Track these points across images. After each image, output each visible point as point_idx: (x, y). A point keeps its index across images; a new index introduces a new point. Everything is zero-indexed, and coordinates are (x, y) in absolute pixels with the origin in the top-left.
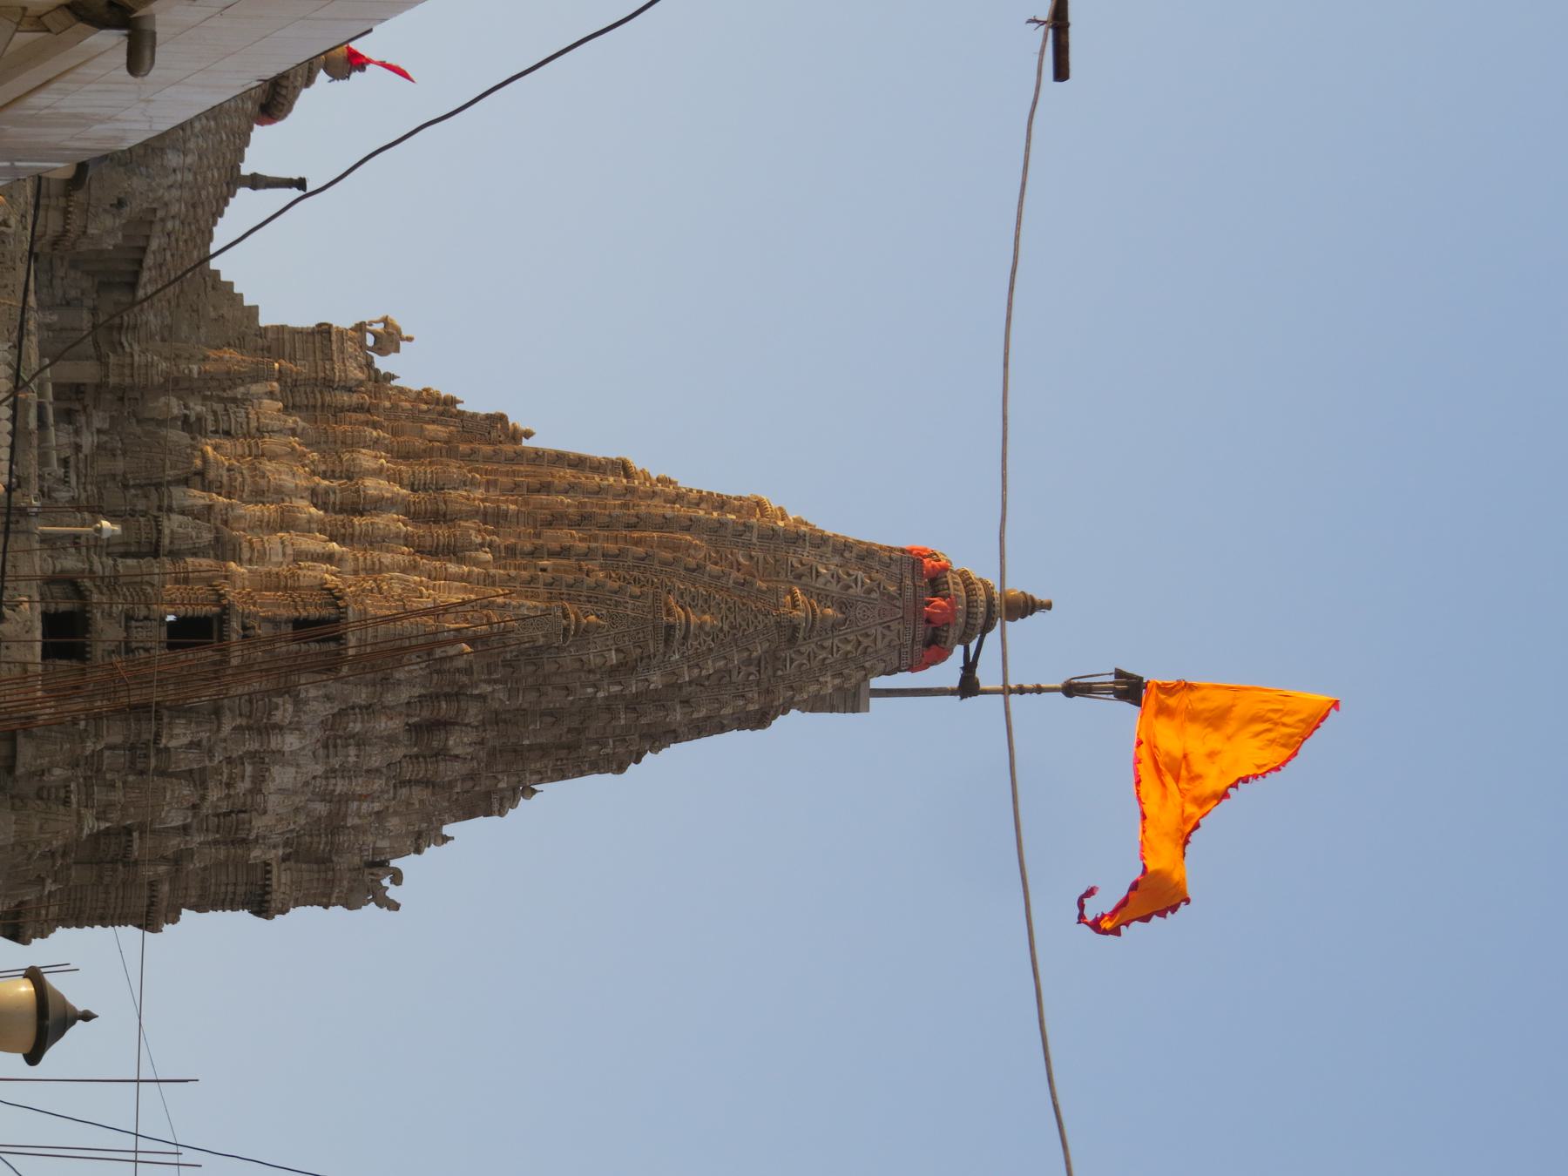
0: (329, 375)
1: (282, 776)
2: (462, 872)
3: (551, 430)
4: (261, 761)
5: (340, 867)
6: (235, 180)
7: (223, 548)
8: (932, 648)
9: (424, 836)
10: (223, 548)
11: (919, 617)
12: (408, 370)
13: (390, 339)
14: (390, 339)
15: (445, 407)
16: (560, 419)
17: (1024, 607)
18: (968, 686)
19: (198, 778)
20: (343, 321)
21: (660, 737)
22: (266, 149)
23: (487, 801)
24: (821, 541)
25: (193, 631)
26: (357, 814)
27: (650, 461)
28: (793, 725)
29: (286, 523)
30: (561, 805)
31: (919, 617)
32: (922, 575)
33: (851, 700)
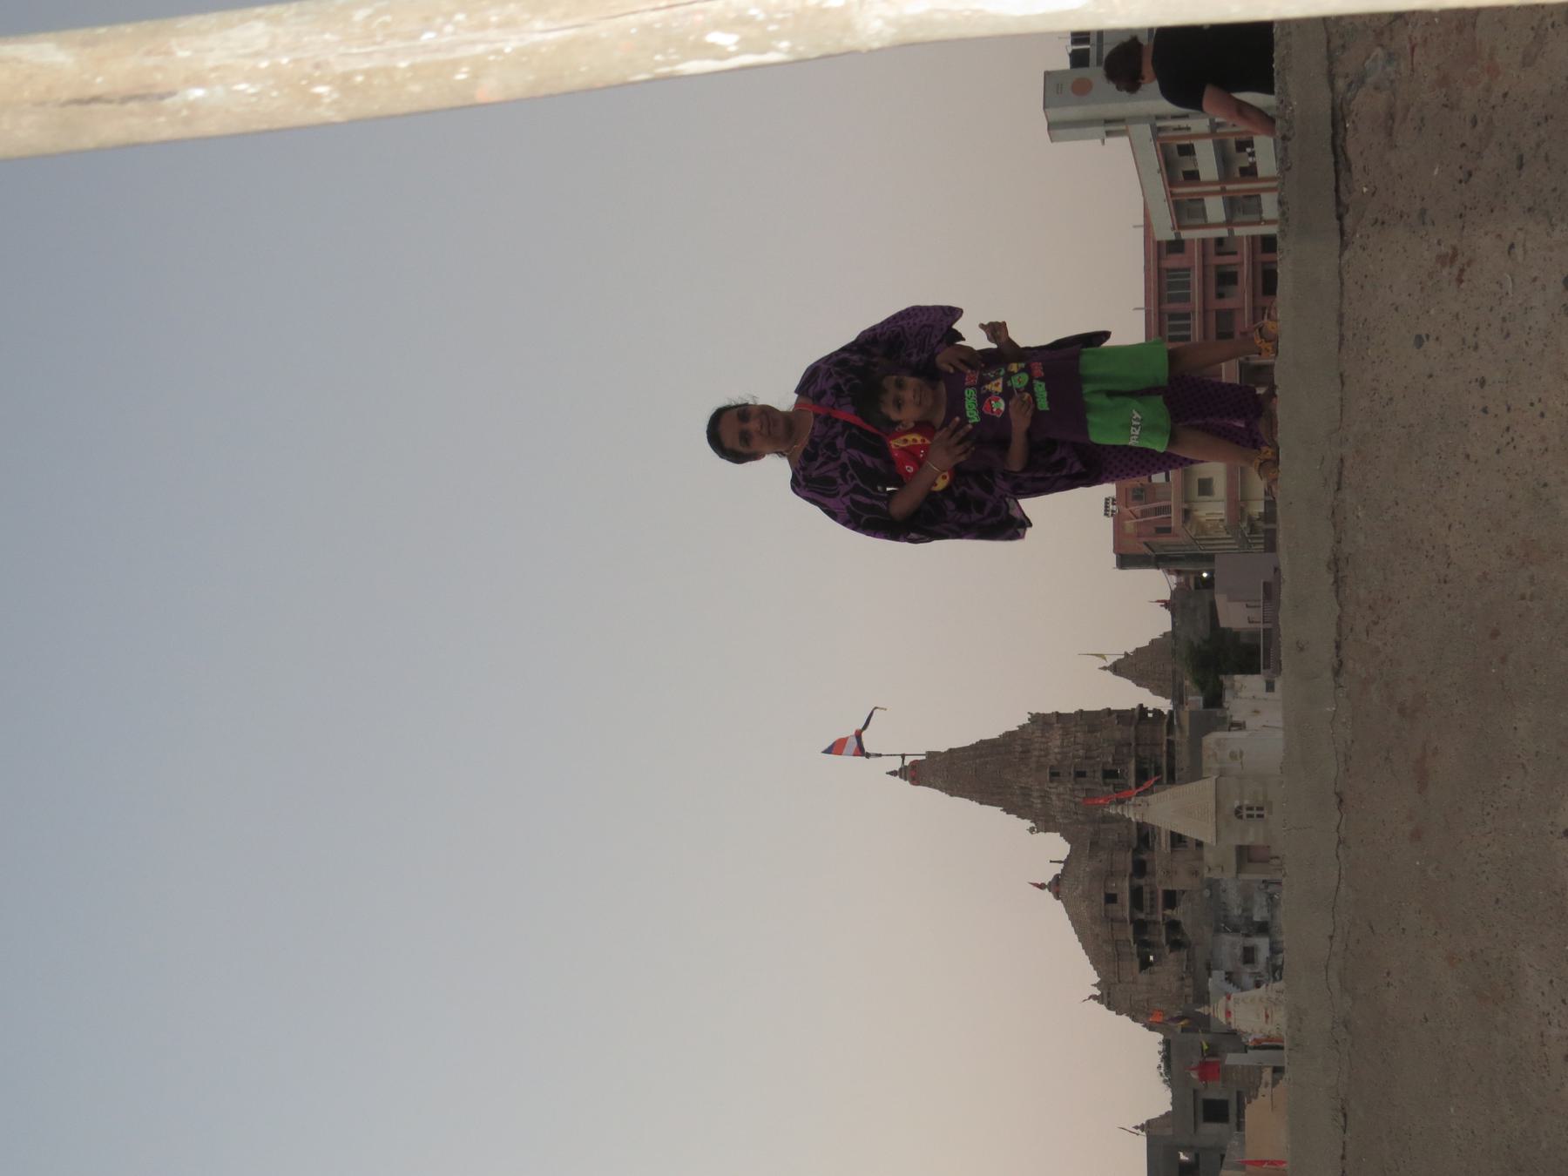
0: (1044, 822)
1: (1058, 742)
2: (1012, 719)
3: (997, 810)
4: (1062, 746)
5: (1041, 722)
6: (1066, 862)
7: (1073, 790)
8: (914, 764)
9: (1023, 728)
10: (1073, 790)
11: (918, 772)
12: (1028, 824)
13: (1031, 830)
14: (1031, 830)
15: (1021, 816)
16: (995, 813)
17: (893, 773)
18: (903, 756)
19: (1075, 743)
20: (1041, 834)
21: (972, 747)
22: (1058, 869)
23: (1009, 734)
24: (941, 790)
25: (1080, 774)
26: (1038, 734)
27: (975, 804)
28: (943, 749)
29: (1059, 795)
30: (993, 732)
31: (918, 772)
32: (915, 781)
33: (930, 755)
